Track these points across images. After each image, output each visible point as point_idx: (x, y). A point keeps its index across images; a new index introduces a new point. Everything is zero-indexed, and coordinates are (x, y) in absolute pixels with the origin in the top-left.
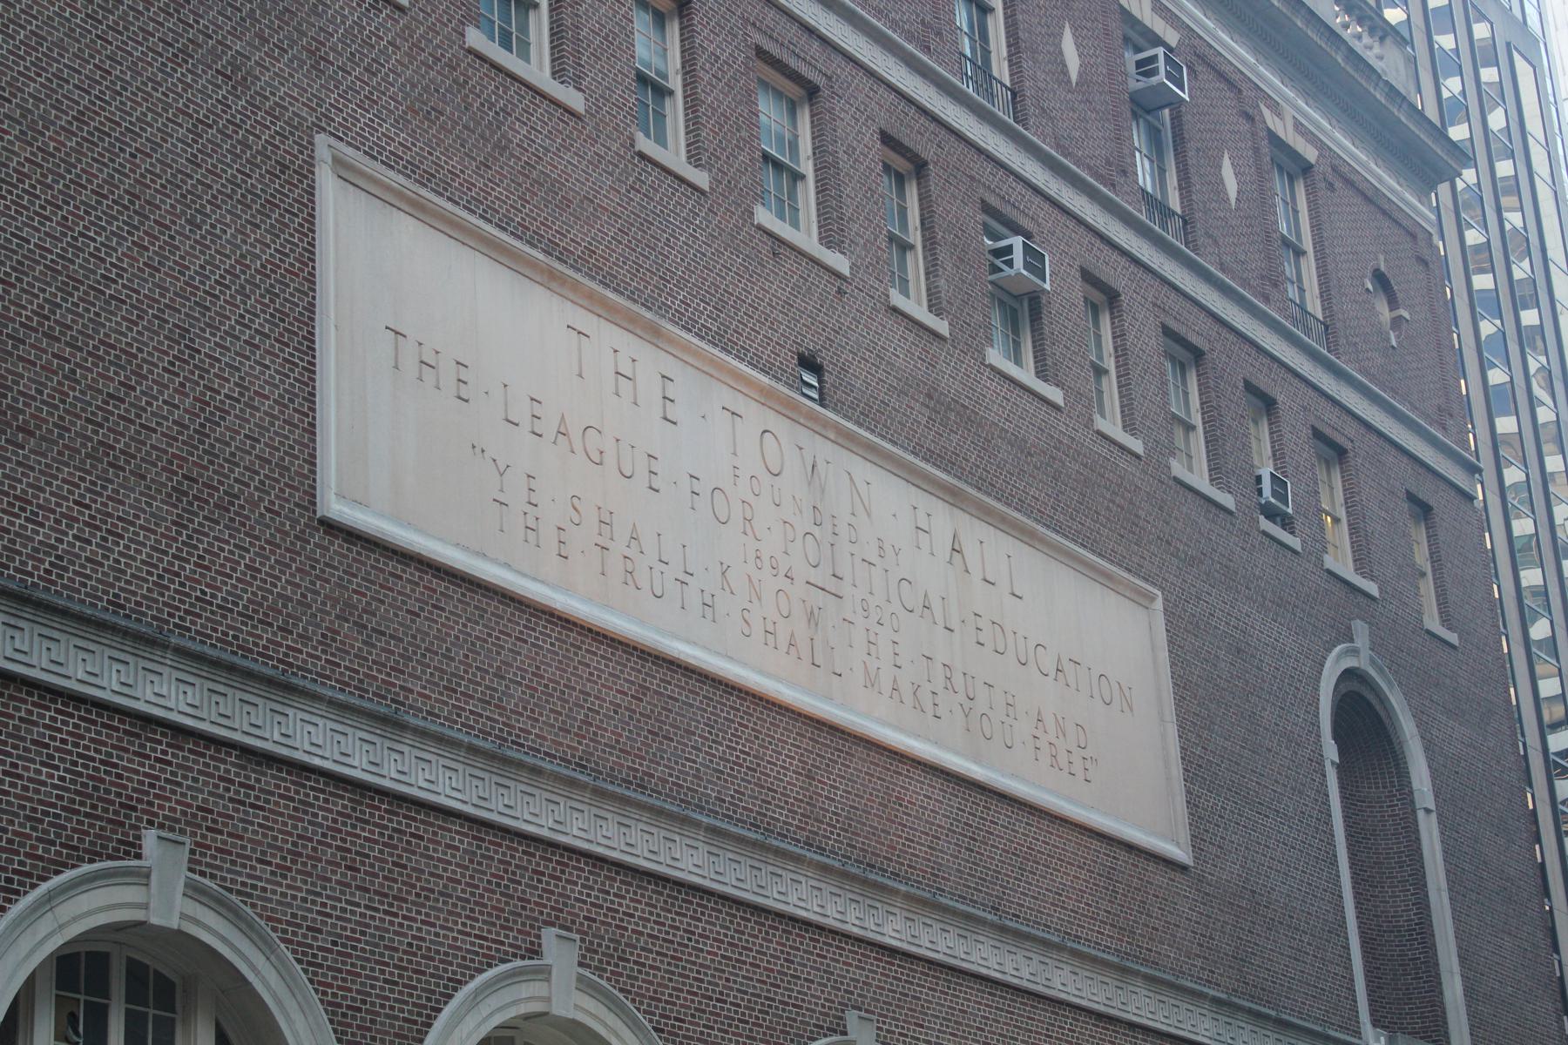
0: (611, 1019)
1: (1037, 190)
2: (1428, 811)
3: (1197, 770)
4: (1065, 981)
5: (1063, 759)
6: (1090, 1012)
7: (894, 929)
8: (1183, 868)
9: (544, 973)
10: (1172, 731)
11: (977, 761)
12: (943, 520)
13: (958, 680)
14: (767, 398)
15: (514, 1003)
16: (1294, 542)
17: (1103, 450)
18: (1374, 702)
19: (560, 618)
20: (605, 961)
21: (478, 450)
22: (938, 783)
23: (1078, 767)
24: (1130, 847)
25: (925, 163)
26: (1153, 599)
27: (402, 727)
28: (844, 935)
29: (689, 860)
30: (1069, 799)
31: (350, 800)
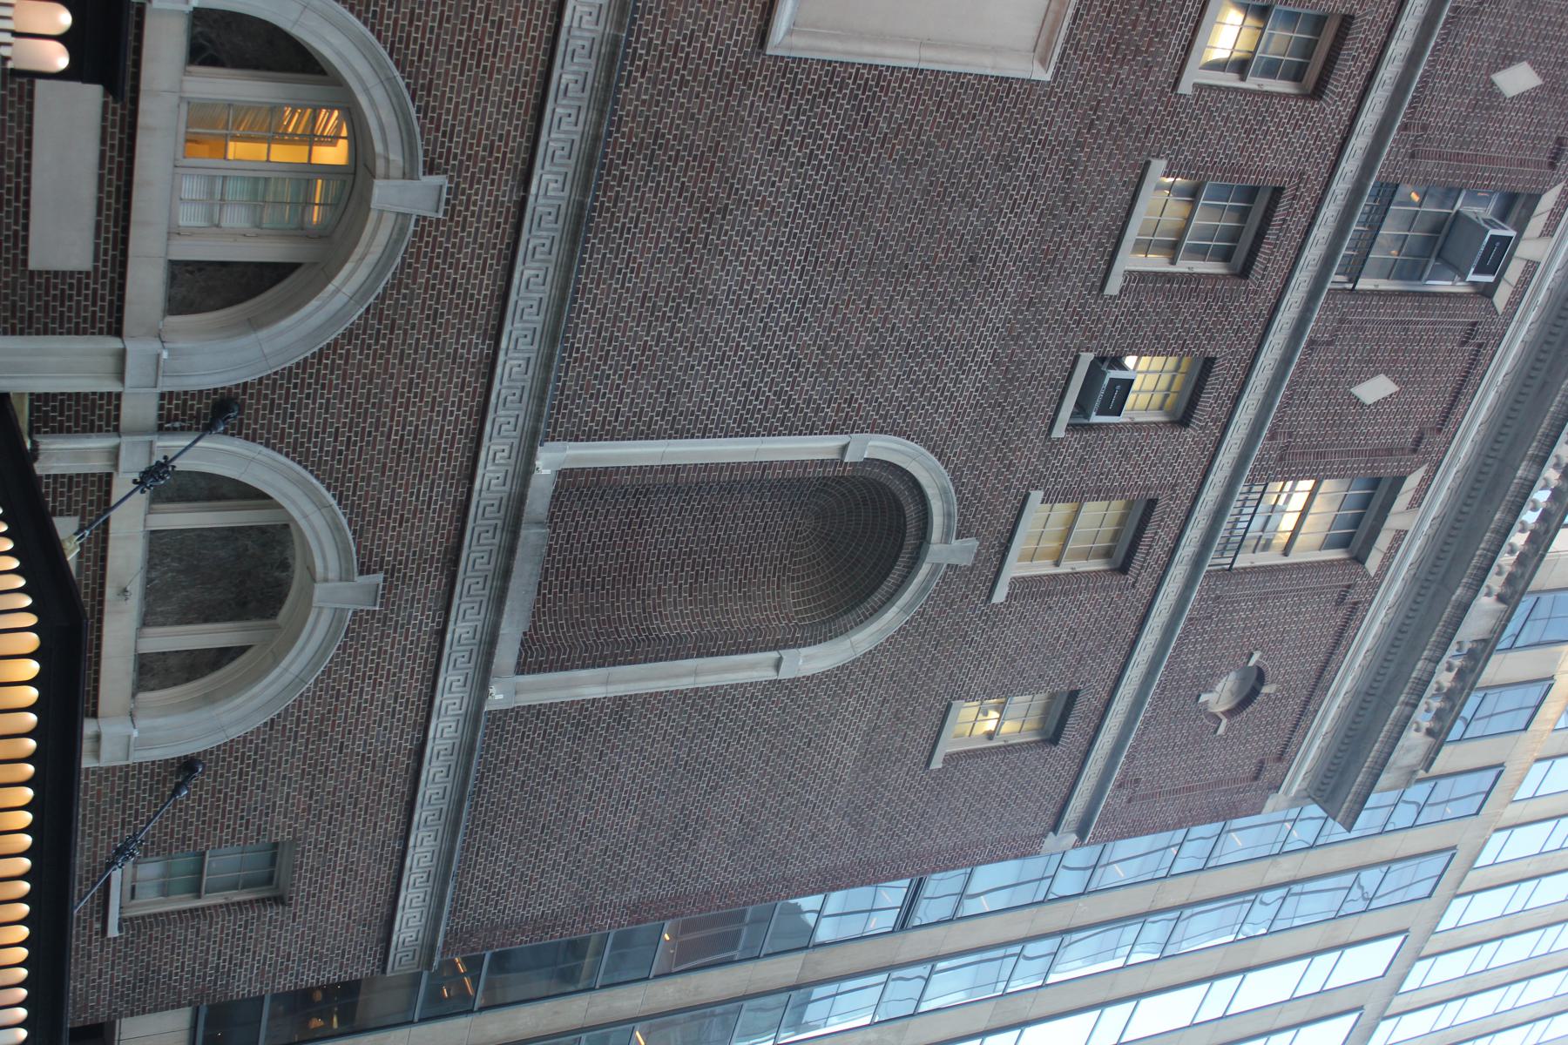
2: (777, 665)
16: (1059, 432)
18: (886, 587)
26: (1044, 62)
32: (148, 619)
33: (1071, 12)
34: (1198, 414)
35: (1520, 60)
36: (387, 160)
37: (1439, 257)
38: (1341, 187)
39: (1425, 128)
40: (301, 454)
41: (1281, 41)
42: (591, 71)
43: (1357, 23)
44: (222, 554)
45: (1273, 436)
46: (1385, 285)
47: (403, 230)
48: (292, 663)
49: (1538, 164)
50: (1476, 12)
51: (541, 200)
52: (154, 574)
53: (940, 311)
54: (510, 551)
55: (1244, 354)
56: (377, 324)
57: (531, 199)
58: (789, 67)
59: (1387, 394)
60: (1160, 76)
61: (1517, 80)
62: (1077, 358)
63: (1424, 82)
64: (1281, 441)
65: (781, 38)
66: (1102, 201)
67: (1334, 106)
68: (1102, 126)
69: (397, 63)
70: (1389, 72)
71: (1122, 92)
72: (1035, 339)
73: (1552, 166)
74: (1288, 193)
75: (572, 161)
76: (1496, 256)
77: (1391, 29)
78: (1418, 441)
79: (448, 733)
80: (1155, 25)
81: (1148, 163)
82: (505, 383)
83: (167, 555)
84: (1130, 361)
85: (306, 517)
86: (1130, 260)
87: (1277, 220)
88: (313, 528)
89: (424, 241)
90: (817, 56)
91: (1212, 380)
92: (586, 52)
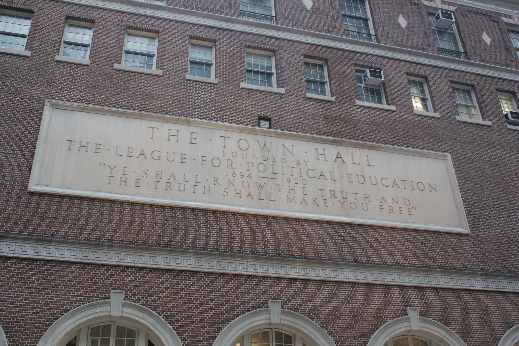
0: (141, 314)
1: (382, 57)
3: (468, 204)
4: (392, 278)
5: (396, 210)
6: (410, 287)
7: (294, 272)
8: (466, 235)
9: (109, 304)
10: (459, 194)
11: (346, 216)
12: (332, 151)
13: (338, 194)
14: (254, 133)
15: (93, 314)
17: (420, 119)
19: (132, 203)
20: (132, 297)
21: (102, 165)
22: (324, 226)
23: (405, 210)
24: (434, 232)
25: (327, 59)
26: (447, 156)
27: (50, 241)
28: (268, 277)
29: (185, 263)
30: (399, 222)
31: (26, 264)
33: (433, 152)
34: (511, 90)
35: (398, 22)
37: (447, 30)
38: (445, 64)
39: (422, 44)
41: (414, 90)
42: (490, 280)
43: (409, 72)
45: (508, 66)
46: (460, 44)
49: (419, 9)
50: (392, 39)
53: (511, 171)
55: (492, 81)
58: (471, 227)
59: (486, 35)
60: (438, 123)
61: (402, 21)
62: (510, 129)
63: (412, 48)
64: (509, 63)
65: (465, 230)
66: (471, 132)
67: (427, 72)
68: (454, 136)
69: (505, 333)
70: (415, 59)
71: (445, 133)
72: (509, 143)
73: (418, 5)
74: (450, 79)
75: (512, 282)
76: (447, 14)
77: (405, 61)
78: (495, 21)
80: (427, 128)
81: (458, 121)
84: (504, 113)
86: (478, 120)
87: (458, 80)
90: (467, 220)
91: (501, 88)
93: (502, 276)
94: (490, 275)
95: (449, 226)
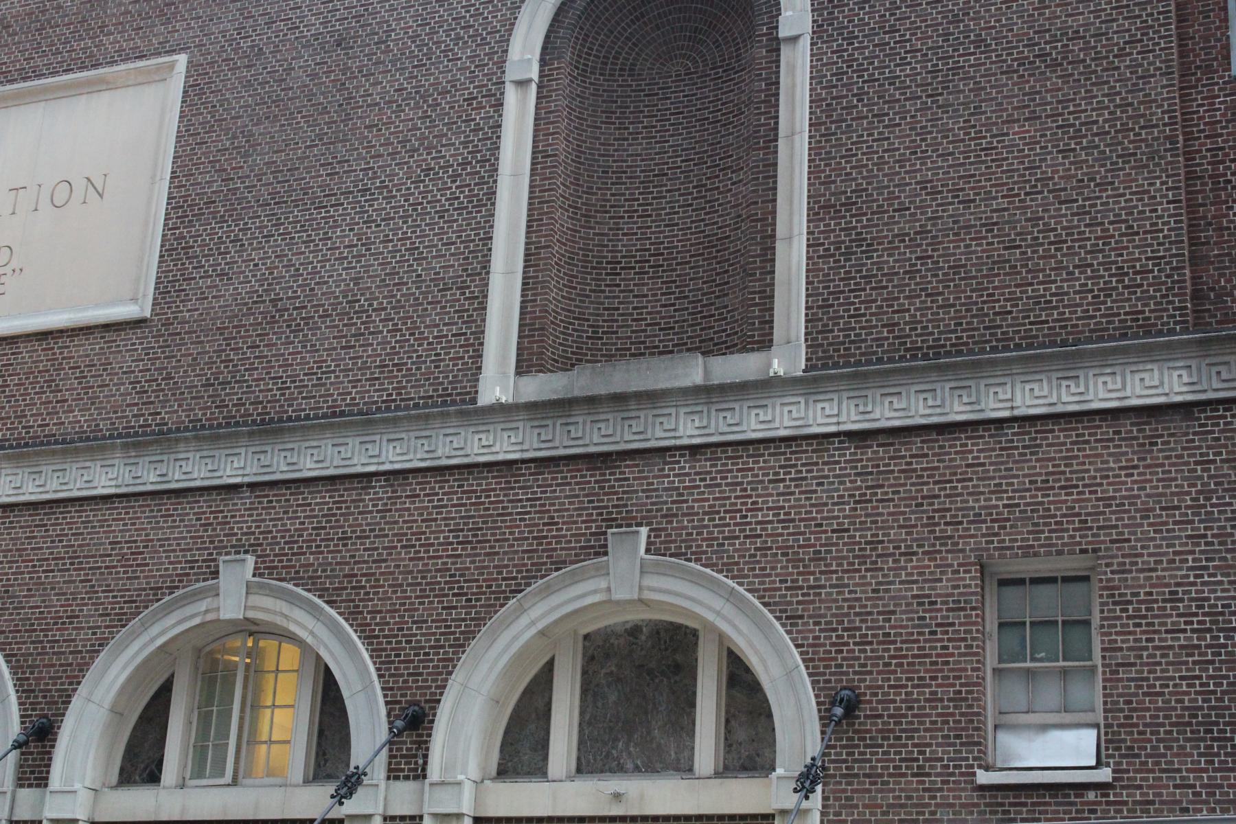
8: (139, 323)
24: (44, 335)
32: (685, 768)
33: (132, 66)
36: (207, 612)
40: (465, 639)
44: (613, 698)
47: (261, 586)
48: (710, 608)
51: (248, 471)
52: (630, 766)
54: (591, 402)
56: (345, 595)
57: (247, 480)
79: (831, 408)
82: (411, 456)
83: (608, 754)
85: (533, 623)
88: (543, 616)
89: (274, 568)
92: (133, 468)
93: (186, 439)
94: (151, 443)
95: (97, 306)
